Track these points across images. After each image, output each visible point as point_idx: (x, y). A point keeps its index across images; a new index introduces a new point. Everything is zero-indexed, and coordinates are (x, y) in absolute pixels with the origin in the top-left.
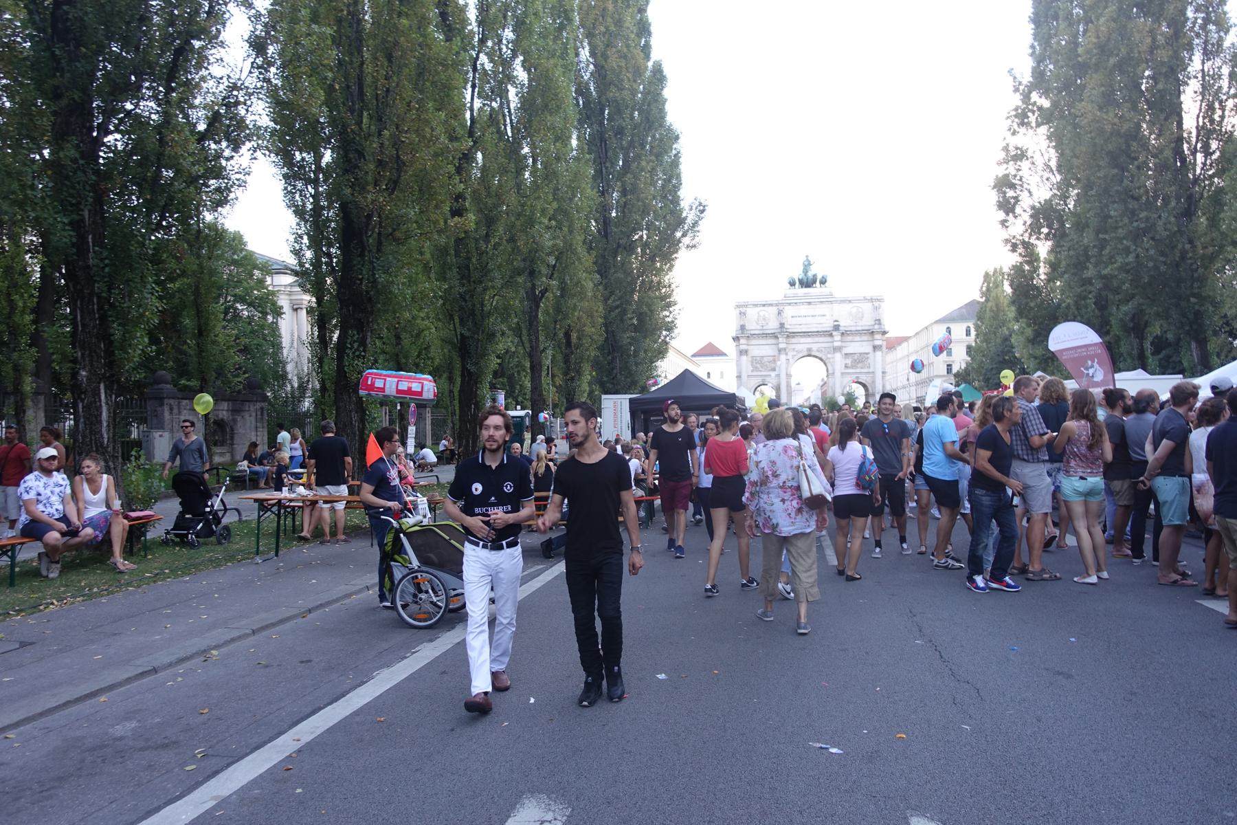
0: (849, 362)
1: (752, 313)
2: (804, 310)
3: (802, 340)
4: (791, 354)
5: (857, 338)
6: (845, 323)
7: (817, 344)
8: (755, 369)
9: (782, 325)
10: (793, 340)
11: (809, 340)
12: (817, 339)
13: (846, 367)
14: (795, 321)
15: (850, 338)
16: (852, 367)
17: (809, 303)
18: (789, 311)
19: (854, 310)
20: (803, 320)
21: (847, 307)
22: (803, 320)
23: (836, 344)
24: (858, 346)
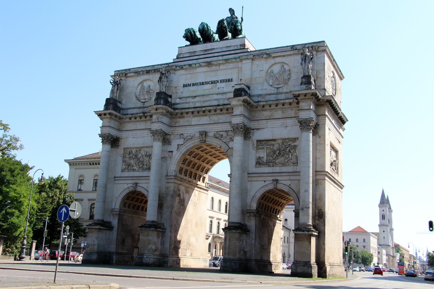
0: (263, 154)
1: (132, 84)
2: (202, 74)
3: (195, 120)
4: (176, 142)
5: (278, 114)
6: (260, 89)
7: (215, 125)
8: (128, 167)
9: (163, 98)
10: (182, 122)
11: (204, 120)
12: (215, 118)
13: (259, 163)
14: (187, 92)
15: (266, 114)
16: (268, 164)
17: (209, 64)
18: (180, 78)
19: (276, 69)
20: (200, 90)
21: (264, 65)
22: (200, 90)
23: (237, 120)
24: (275, 128)
